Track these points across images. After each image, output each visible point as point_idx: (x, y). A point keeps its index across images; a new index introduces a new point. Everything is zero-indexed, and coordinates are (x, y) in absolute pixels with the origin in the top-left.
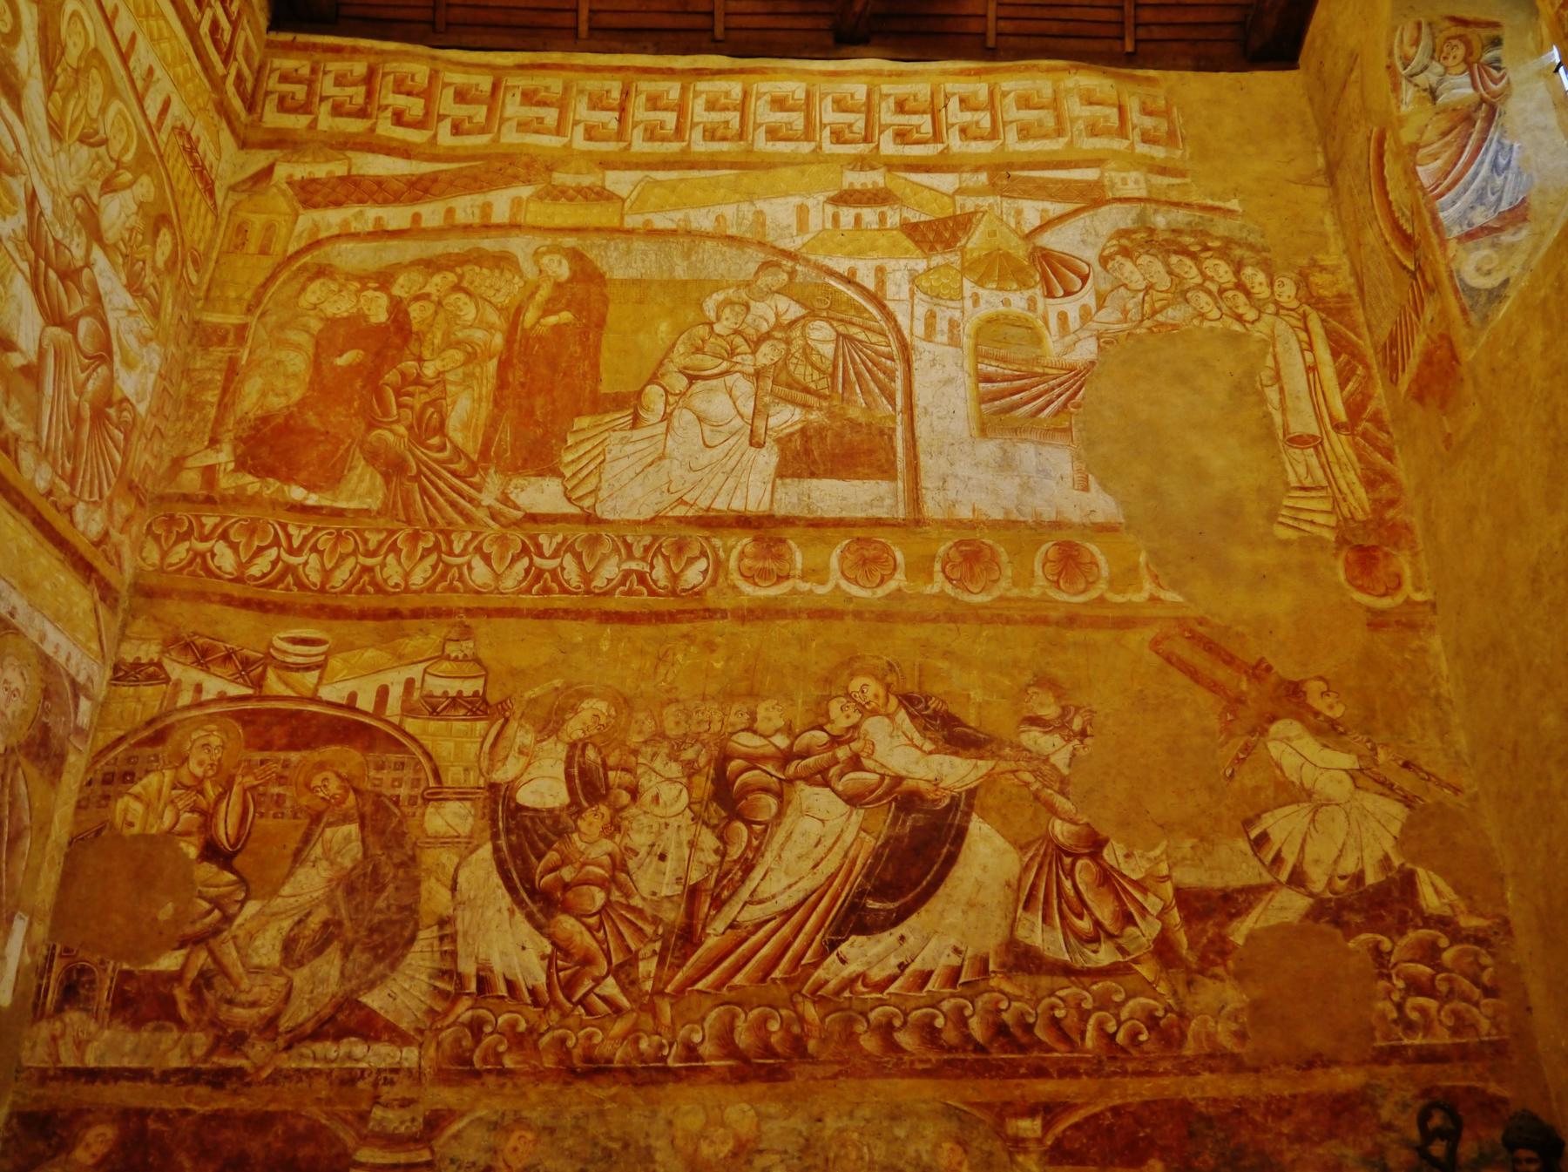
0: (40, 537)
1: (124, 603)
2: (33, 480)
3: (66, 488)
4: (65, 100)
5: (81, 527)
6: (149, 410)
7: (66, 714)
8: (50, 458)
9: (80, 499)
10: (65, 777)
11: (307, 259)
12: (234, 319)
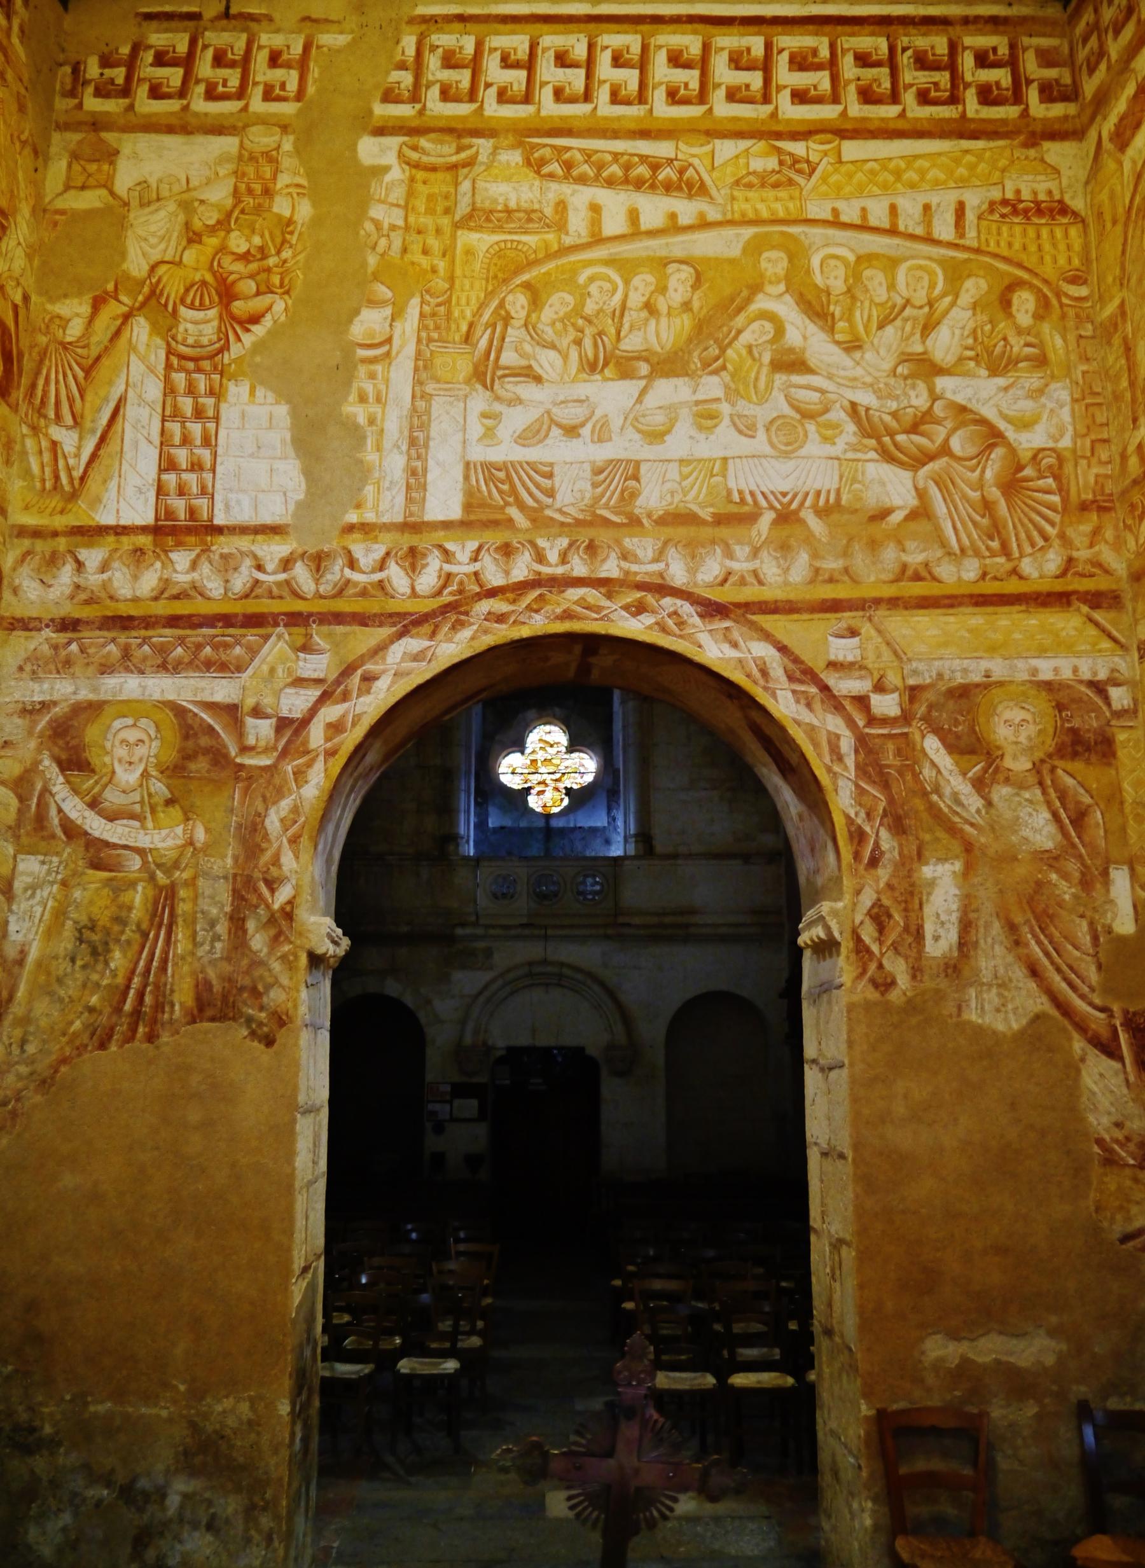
0: (990, 609)
1: (1127, 598)
2: (960, 579)
3: (1001, 560)
4: (850, 320)
5: (1035, 575)
6: (1076, 435)
7: (1097, 709)
8: (970, 552)
9: (1021, 556)
10: (1121, 753)
11: (1138, 199)
12: (1116, 302)
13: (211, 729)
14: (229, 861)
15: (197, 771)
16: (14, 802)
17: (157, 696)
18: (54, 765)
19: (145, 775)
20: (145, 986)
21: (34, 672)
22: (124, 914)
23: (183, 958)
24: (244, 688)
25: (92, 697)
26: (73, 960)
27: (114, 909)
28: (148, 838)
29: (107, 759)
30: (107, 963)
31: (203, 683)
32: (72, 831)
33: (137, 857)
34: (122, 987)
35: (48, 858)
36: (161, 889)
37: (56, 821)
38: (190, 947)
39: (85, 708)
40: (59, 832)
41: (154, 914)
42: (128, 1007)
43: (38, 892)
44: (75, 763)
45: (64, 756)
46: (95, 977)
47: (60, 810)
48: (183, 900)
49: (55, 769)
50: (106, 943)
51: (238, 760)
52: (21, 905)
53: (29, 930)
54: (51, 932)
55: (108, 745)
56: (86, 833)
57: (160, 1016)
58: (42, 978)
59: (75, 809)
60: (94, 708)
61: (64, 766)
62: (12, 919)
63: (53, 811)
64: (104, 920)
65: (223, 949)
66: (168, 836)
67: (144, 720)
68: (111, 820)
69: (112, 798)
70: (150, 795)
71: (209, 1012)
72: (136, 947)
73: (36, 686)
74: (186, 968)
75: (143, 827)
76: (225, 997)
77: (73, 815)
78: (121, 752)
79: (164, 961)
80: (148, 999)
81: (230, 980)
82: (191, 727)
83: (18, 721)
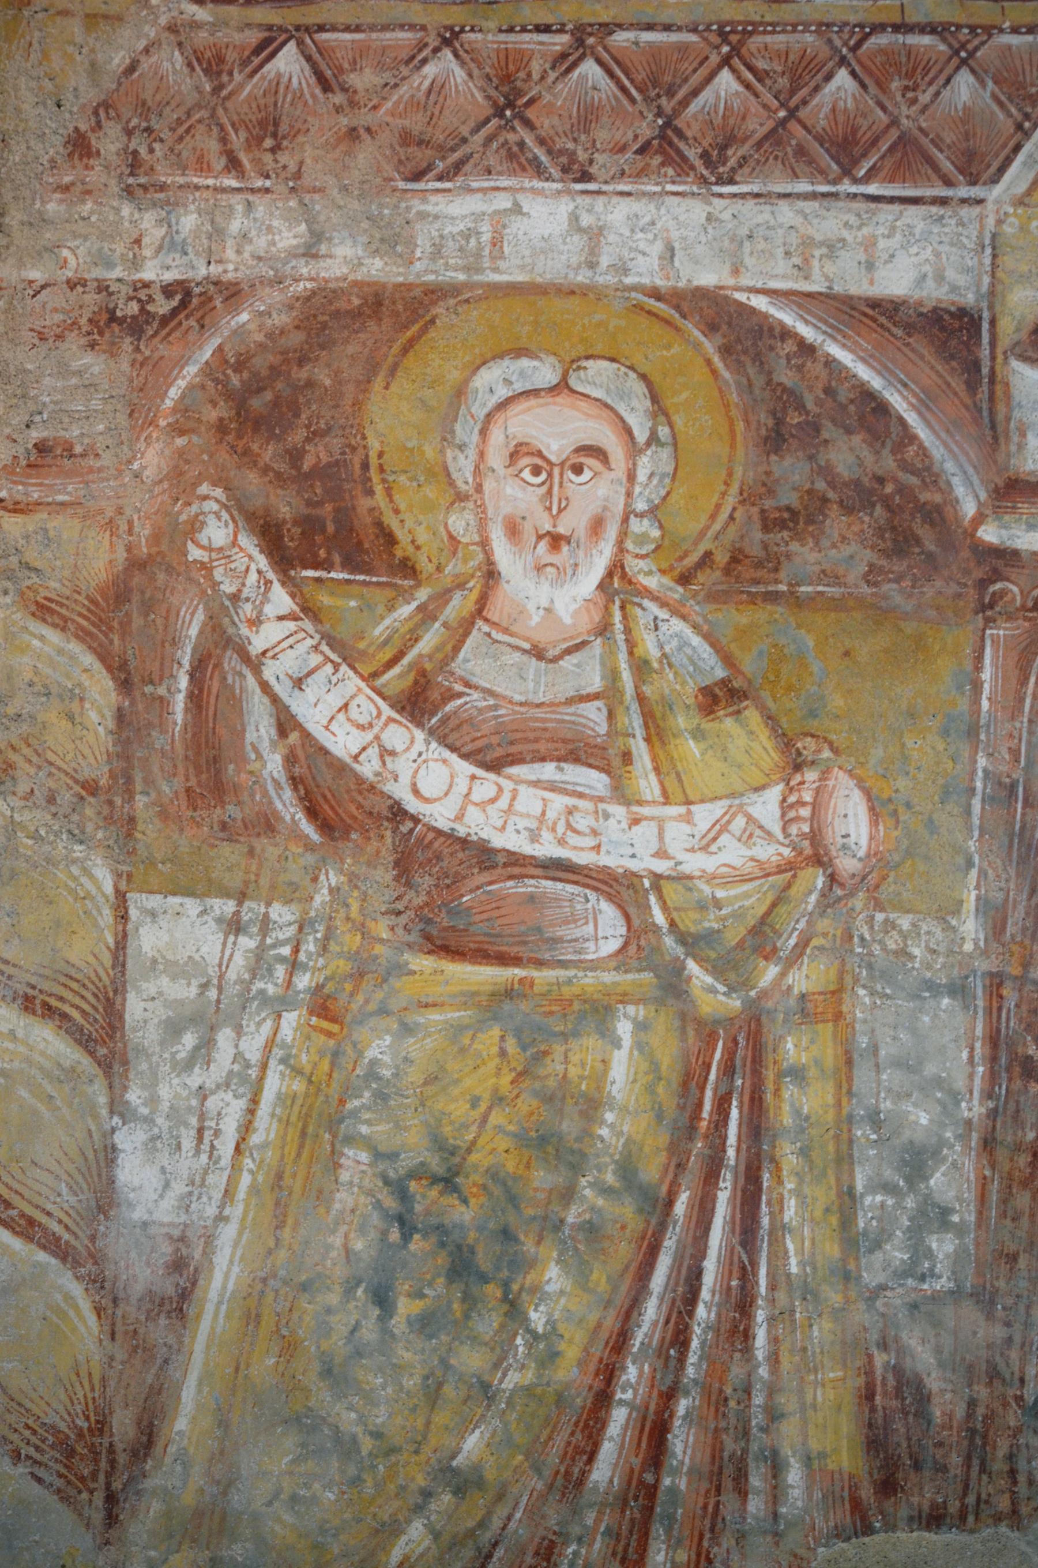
13: (872, 411)
14: (970, 928)
15: (825, 576)
16: (101, 691)
17: (646, 270)
18: (248, 542)
19: (617, 583)
20: (669, 1396)
21: (135, 163)
22: (569, 1126)
23: (809, 1293)
24: (996, 245)
25: (377, 269)
26: (382, 1300)
27: (526, 1103)
28: (645, 835)
29: (460, 523)
30: (513, 1309)
31: (831, 223)
32: (337, 804)
33: (608, 911)
34: (581, 1400)
35: (252, 909)
36: (708, 1032)
37: (274, 764)
38: (833, 1250)
39: (357, 314)
40: (287, 806)
41: (688, 1125)
42: (604, 1471)
43: (224, 1037)
44: (331, 534)
45: (286, 506)
46: (471, 1360)
47: (286, 723)
48: (798, 1074)
49: (253, 559)
50: (506, 1234)
51: (989, 534)
52: (162, 1087)
53: (198, 1183)
54: (287, 1197)
55: (462, 468)
56: (398, 812)
57: (729, 1501)
58: (264, 1365)
59: (344, 717)
60: (397, 316)
61: (289, 548)
62: (129, 1140)
63: (260, 727)
64: (493, 1149)
65: (958, 1258)
66: (721, 827)
67: (597, 367)
68: (494, 766)
69: (493, 675)
70: (641, 667)
71: (924, 1493)
72: (624, 1251)
73: (148, 220)
74: (822, 1331)
75: (621, 793)
76: (977, 1437)
77: (343, 742)
78: (514, 494)
79: (742, 1303)
80: (683, 1444)
81: (994, 1375)
82: (786, 399)
83: (93, 364)
